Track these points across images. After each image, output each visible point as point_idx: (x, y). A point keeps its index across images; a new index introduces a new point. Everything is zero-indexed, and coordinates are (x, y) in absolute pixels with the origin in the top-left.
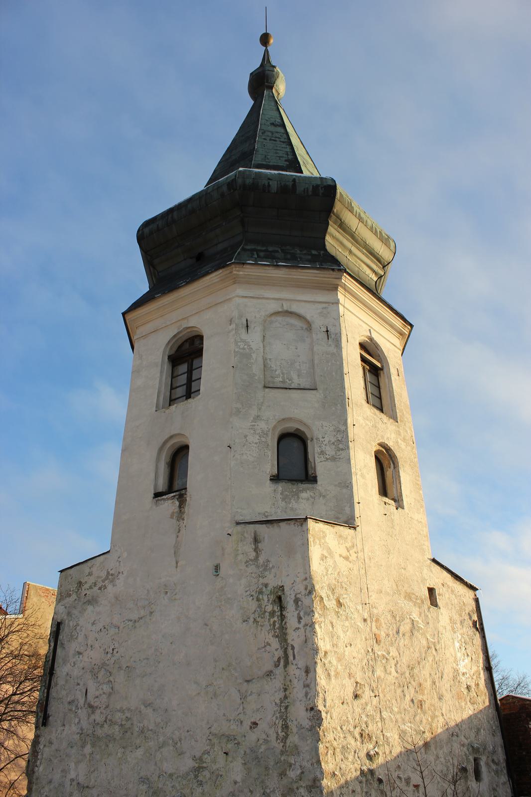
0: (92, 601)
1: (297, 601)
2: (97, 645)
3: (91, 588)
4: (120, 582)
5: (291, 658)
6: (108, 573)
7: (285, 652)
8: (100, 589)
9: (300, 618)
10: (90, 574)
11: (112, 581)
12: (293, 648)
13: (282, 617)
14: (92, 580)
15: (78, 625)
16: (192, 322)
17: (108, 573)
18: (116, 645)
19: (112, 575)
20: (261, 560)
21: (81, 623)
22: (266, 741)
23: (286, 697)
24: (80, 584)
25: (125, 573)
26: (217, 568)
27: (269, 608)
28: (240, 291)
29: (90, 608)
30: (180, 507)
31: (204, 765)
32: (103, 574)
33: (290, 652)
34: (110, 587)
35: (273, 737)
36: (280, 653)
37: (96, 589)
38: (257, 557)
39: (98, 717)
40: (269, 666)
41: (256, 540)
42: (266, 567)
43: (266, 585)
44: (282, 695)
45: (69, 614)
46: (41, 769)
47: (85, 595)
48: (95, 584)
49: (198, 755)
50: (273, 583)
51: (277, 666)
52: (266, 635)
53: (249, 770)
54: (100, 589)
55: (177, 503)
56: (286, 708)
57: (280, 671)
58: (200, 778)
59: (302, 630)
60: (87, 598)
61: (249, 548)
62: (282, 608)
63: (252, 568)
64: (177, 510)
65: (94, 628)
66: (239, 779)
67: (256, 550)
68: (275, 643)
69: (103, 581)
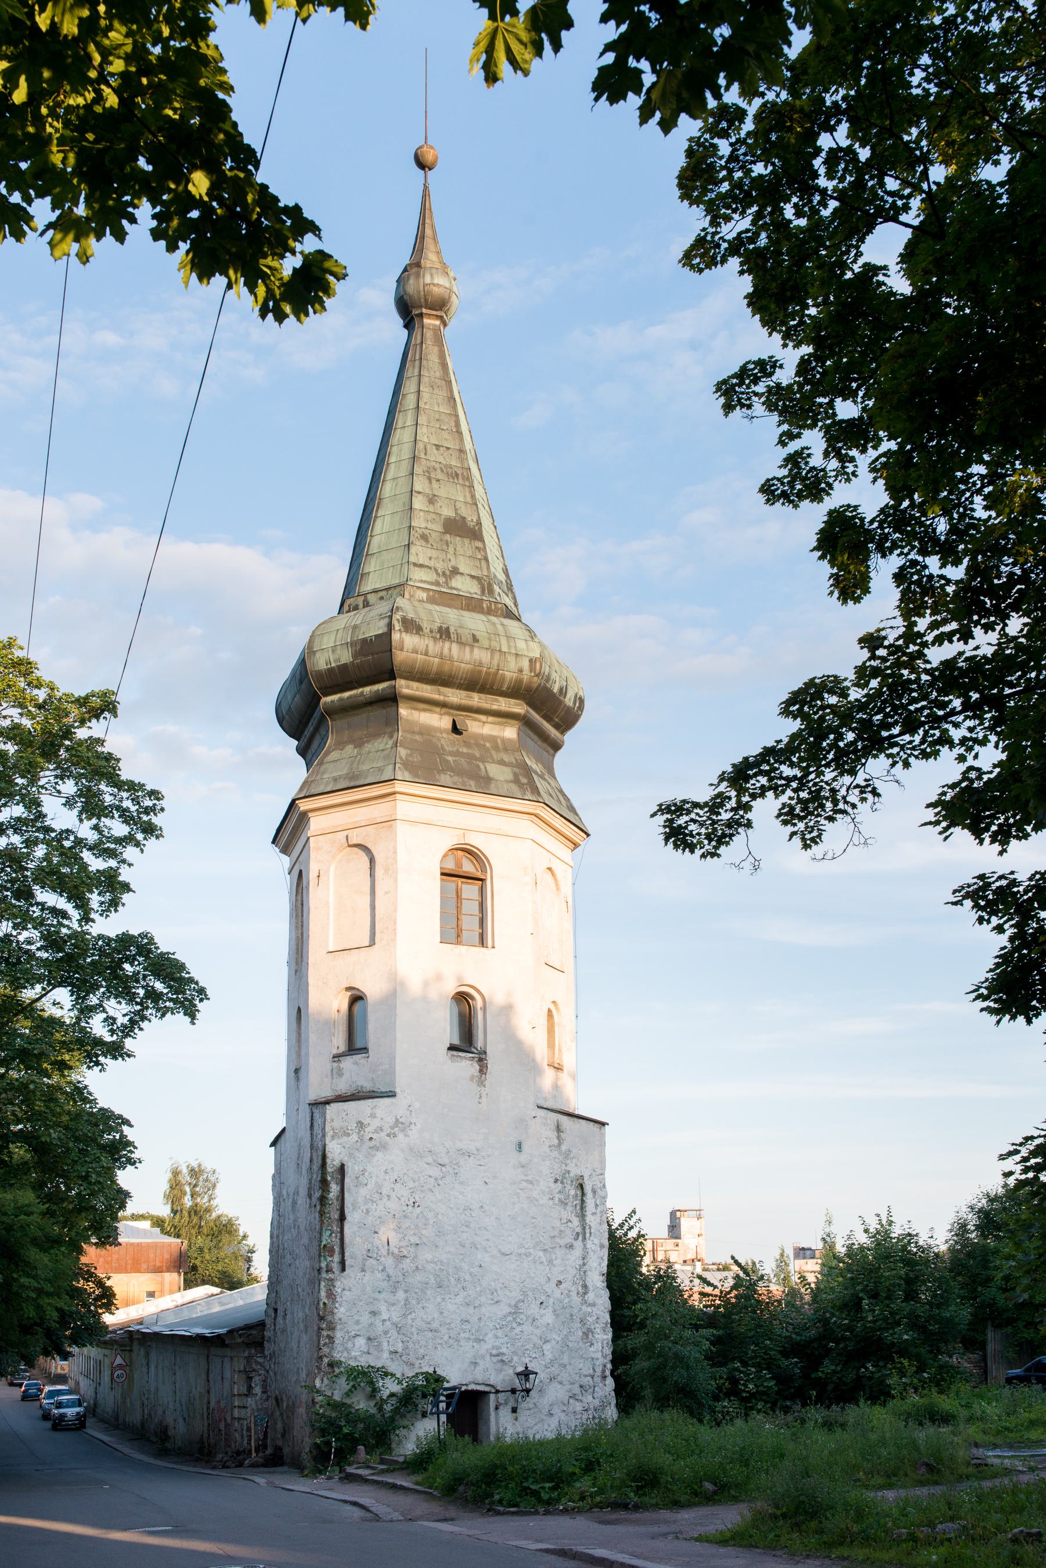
0: (383, 1147)
2: (393, 1195)
3: (376, 1131)
4: (414, 1132)
5: (588, 1235)
6: (397, 1120)
7: (584, 1229)
8: (388, 1135)
9: (597, 1205)
10: (373, 1116)
11: (403, 1131)
12: (590, 1228)
13: (583, 1201)
14: (375, 1123)
15: (364, 1170)
16: (476, 841)
17: (397, 1120)
18: (418, 1199)
19: (402, 1123)
20: (564, 1148)
21: (369, 1168)
22: (569, 1296)
23: (584, 1264)
24: (361, 1125)
25: (419, 1126)
26: (520, 1145)
27: (572, 1192)
29: (379, 1155)
30: (481, 1071)
32: (391, 1120)
33: (587, 1231)
34: (401, 1136)
35: (574, 1294)
36: (579, 1230)
37: (383, 1134)
38: (560, 1144)
39: (407, 1264)
40: (569, 1239)
41: (559, 1129)
42: (567, 1155)
43: (569, 1172)
44: (581, 1262)
45: (351, 1155)
46: (342, 1310)
47: (371, 1139)
48: (382, 1130)
49: (513, 1303)
50: (575, 1172)
51: (576, 1239)
52: (568, 1212)
53: (557, 1316)
54: (388, 1135)
55: (478, 1067)
56: (585, 1272)
57: (578, 1244)
58: (518, 1320)
59: (599, 1215)
60: (373, 1143)
62: (583, 1194)
63: (555, 1154)
64: (477, 1074)
65: (387, 1178)
66: (550, 1322)
67: (558, 1137)
68: (576, 1222)
69: (392, 1128)
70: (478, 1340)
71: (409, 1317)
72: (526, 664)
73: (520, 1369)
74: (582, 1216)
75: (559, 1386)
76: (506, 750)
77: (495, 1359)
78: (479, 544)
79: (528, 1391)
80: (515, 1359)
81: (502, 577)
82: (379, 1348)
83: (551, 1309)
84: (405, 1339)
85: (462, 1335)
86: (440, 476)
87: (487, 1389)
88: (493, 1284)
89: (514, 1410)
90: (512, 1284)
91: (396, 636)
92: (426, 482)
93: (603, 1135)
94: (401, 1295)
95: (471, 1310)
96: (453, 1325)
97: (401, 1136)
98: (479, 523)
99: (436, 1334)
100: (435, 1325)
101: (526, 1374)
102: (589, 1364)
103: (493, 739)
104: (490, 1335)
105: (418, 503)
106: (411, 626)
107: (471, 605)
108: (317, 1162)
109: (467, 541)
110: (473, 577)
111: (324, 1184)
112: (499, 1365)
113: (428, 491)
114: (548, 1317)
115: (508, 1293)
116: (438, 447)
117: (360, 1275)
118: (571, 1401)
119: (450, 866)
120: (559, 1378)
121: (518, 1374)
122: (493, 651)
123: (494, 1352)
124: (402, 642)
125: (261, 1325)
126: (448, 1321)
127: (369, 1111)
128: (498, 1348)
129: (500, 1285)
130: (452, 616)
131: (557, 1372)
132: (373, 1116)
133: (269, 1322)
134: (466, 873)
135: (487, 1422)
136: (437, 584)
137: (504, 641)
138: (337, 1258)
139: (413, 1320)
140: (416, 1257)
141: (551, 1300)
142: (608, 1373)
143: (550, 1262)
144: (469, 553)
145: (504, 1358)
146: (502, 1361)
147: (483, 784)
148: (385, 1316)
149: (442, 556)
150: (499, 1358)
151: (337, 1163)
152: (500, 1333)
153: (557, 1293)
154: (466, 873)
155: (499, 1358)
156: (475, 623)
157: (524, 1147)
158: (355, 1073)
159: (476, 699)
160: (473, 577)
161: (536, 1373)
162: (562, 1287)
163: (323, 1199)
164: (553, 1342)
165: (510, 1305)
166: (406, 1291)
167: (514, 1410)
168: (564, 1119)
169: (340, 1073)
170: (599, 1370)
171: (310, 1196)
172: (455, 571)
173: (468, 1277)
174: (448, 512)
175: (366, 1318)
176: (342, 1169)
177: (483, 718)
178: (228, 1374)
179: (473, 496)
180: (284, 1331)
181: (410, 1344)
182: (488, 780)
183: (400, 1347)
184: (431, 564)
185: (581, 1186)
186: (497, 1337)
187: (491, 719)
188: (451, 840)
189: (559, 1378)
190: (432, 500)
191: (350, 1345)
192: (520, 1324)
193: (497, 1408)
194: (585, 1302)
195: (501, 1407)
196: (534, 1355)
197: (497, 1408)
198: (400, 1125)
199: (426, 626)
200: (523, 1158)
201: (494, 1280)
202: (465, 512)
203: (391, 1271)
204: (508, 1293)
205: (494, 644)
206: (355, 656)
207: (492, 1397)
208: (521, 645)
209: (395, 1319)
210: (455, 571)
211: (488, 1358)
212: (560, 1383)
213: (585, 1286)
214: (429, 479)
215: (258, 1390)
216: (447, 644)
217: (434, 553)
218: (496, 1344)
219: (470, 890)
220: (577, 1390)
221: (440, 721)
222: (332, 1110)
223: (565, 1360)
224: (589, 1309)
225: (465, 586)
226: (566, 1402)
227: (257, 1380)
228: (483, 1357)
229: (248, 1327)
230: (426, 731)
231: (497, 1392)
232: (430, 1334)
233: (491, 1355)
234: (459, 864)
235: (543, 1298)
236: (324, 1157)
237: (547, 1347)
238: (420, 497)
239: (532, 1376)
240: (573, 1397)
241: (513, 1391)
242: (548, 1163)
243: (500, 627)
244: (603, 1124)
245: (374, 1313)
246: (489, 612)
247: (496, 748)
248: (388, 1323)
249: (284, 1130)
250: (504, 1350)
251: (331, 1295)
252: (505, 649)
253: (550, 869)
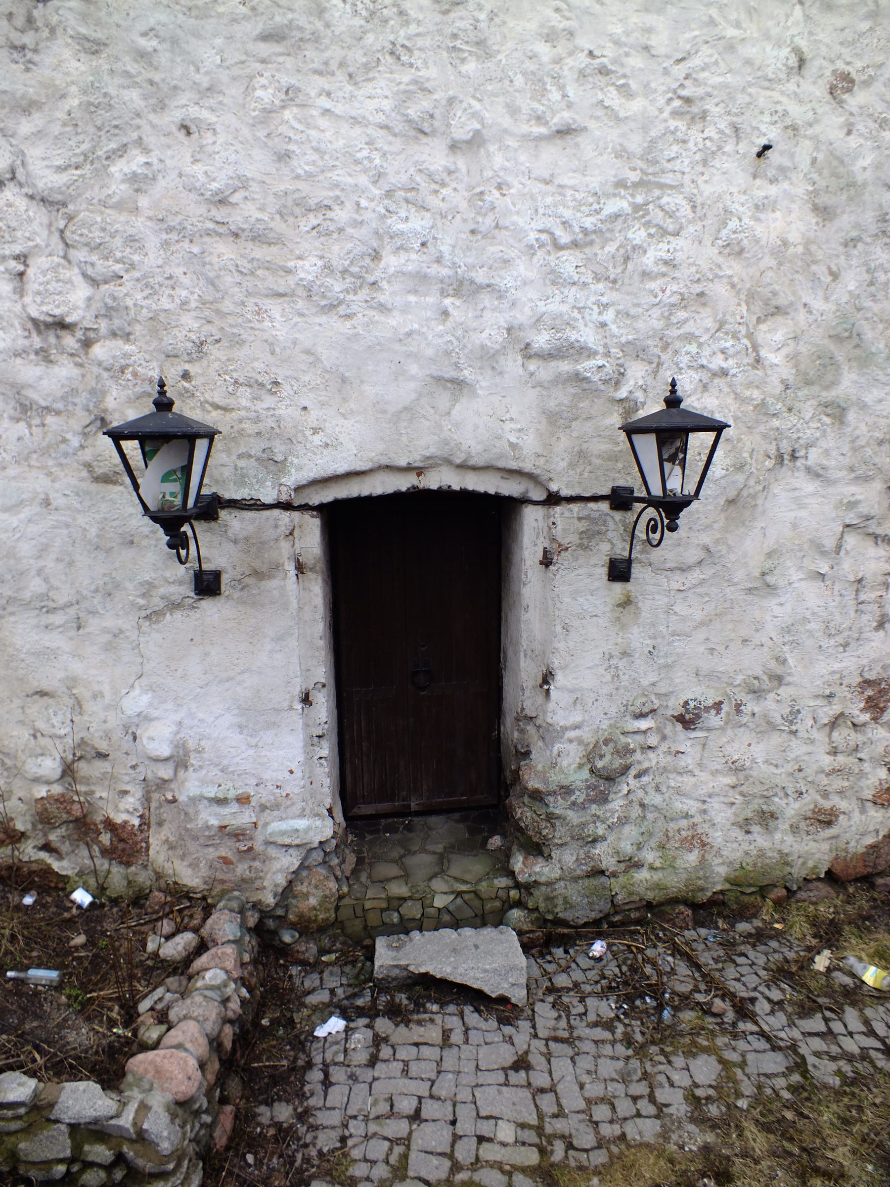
31: (668, 179)
70: (463, 288)
71: (119, 168)
75: (809, 486)
77: (545, 371)
79: (672, 507)
80: (637, 373)
83: (801, 189)
84: (102, 267)
85: (391, 261)
87: (510, 488)
88: (543, 50)
89: (619, 571)
90: (636, 61)
95: (434, 155)
96: (342, 215)
99: (261, 253)
100: (246, 213)
101: (672, 429)
104: (523, 269)
112: (561, 397)
114: (790, 223)
115: (613, 98)
118: (851, 540)
120: (814, 457)
123: (541, 340)
126: (322, 194)
128: (558, 324)
129: (582, 60)
131: (809, 433)
139: (139, 182)
141: (804, 153)
145: (587, 366)
146: (578, 378)
150: (565, 367)
152: (568, 263)
155: (565, 367)
161: (718, 428)
162: (856, 100)
164: (802, 316)
165: (621, 153)
167: (619, 571)
183: (76, 301)
189: (814, 457)
192: (664, 232)
195: (562, 560)
196: (718, 362)
197: (547, 561)
201: (550, 37)
204: (613, 98)
207: (532, 520)
209: (47, 179)
211: (513, 364)
212: (814, 473)
218: (554, 307)
226: (829, 543)
228: (488, 358)
231: (553, 499)
232: (224, 252)
233: (527, 352)
235: (772, 134)
237: (774, 337)
239: (699, 441)
250: (588, 336)
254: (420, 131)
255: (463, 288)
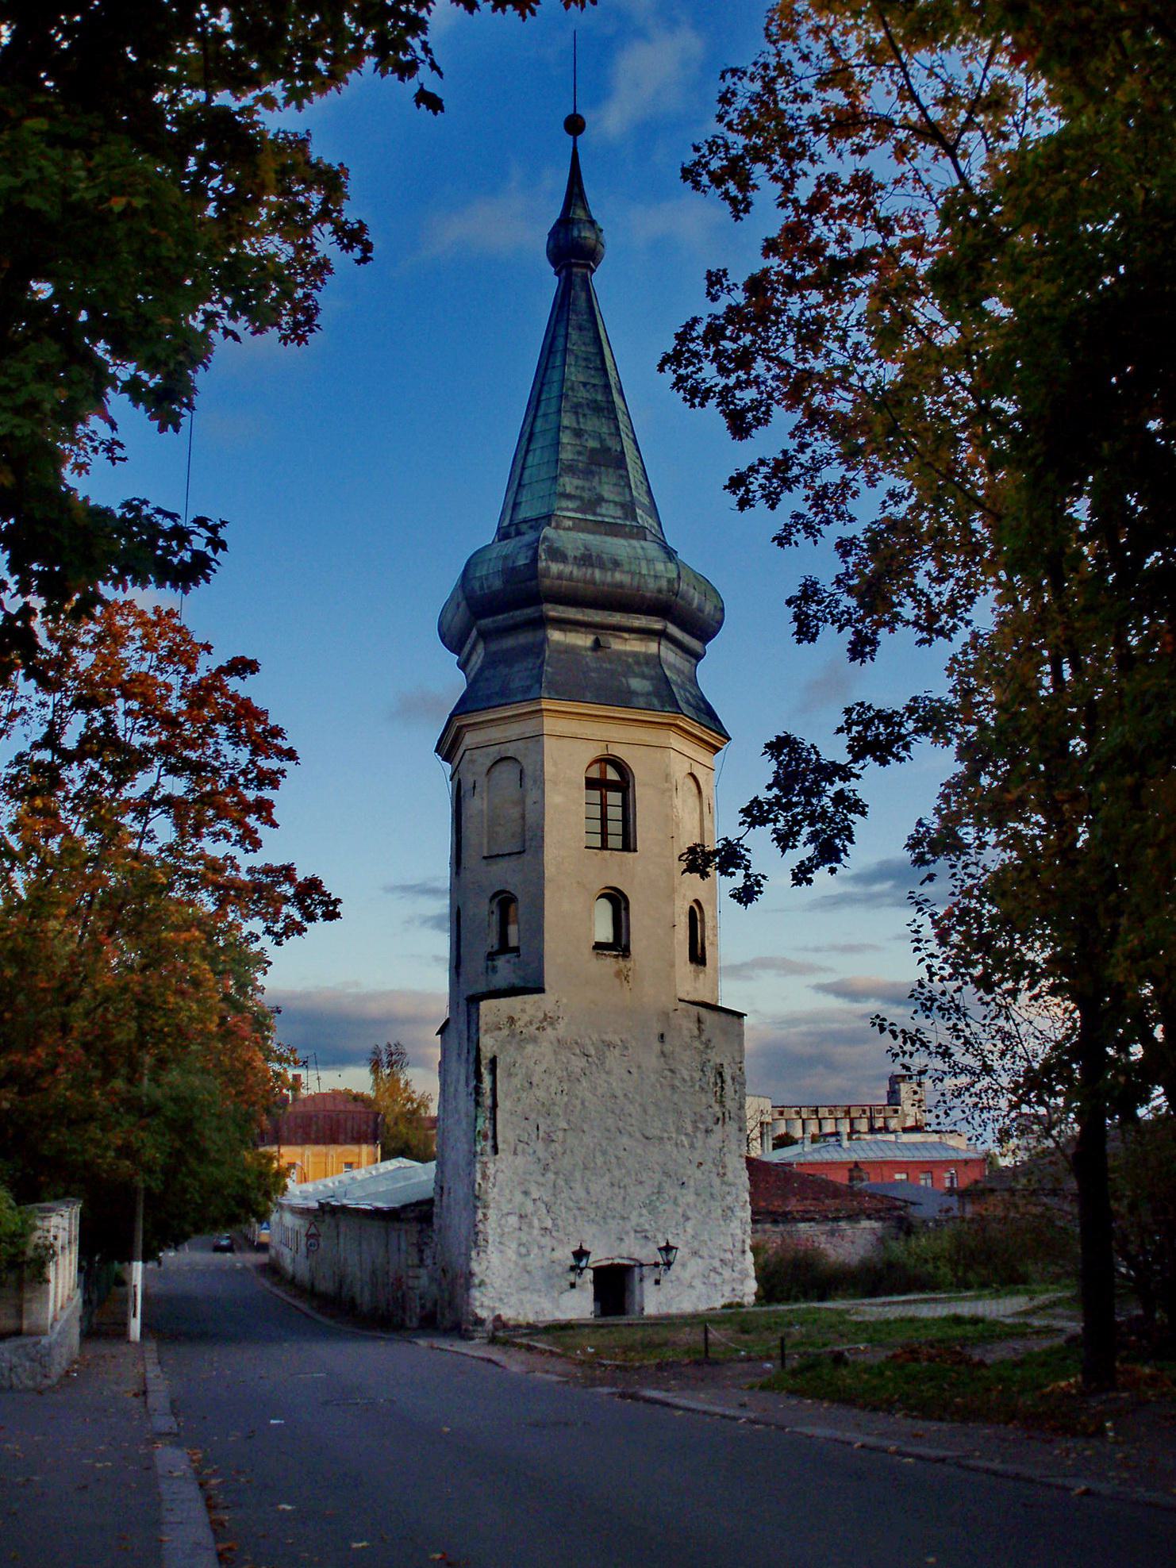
0: (534, 1040)
1: (733, 1079)
4: (561, 1026)
11: (551, 1024)
13: (722, 1088)
14: (526, 1018)
16: (618, 751)
20: (703, 1039)
26: (662, 1036)
27: (712, 1080)
28: (676, 741)
29: (530, 1048)
34: (549, 1030)
37: (533, 1028)
41: (699, 1021)
53: (698, 1195)
61: (694, 1027)
62: (723, 1082)
63: (697, 1044)
68: (717, 1108)
70: (623, 1218)
72: (664, 584)
73: (663, 1244)
74: (722, 1103)
76: (647, 664)
78: (622, 472)
81: (646, 500)
82: (531, 1226)
83: (692, 1190)
86: (587, 411)
89: (657, 1282)
91: (542, 565)
92: (574, 418)
93: (742, 1025)
94: (550, 1176)
97: (549, 1030)
98: (623, 452)
101: (668, 1249)
102: (730, 1239)
103: (635, 654)
104: (635, 1213)
105: (566, 438)
106: (557, 555)
107: (613, 530)
108: (473, 1053)
109: (611, 470)
110: (615, 503)
111: (478, 1076)
112: (643, 1241)
113: (575, 425)
116: (585, 384)
117: (511, 1158)
119: (595, 773)
121: (660, 1249)
122: (632, 573)
124: (548, 568)
125: (430, 1202)
127: (519, 1008)
130: (595, 541)
132: (523, 1011)
133: (437, 1198)
134: (612, 781)
135: (633, 1292)
136: (583, 512)
137: (643, 563)
138: (490, 1143)
140: (564, 1141)
142: (747, 1248)
143: (692, 1146)
144: (614, 480)
147: (623, 698)
148: (535, 1195)
149: (587, 485)
151: (489, 1055)
153: (698, 1174)
154: (612, 781)
156: (618, 547)
157: (667, 1039)
158: (505, 971)
159: (617, 618)
160: (615, 503)
163: (478, 1090)
166: (556, 1173)
167: (657, 1282)
168: (703, 1011)
169: (494, 969)
170: (739, 1245)
171: (467, 1085)
172: (600, 500)
173: (613, 1160)
174: (592, 444)
175: (519, 1197)
176: (493, 1061)
177: (626, 635)
178: (403, 1246)
179: (618, 428)
180: (449, 1208)
181: (560, 1222)
182: (632, 693)
183: (549, 1224)
184: (578, 493)
185: (721, 1074)
186: (641, 1215)
187: (633, 636)
188: (597, 751)
190: (578, 433)
191: (503, 1222)
193: (641, 1280)
194: (723, 1183)
198: (549, 1020)
199: (570, 553)
200: (667, 1048)
202: (611, 443)
203: (540, 1154)
205: (634, 567)
206: (506, 582)
207: (637, 1270)
208: (660, 567)
210: (600, 500)
211: (632, 1234)
213: (724, 1167)
214: (576, 413)
215: (429, 1262)
216: (589, 571)
217: (579, 483)
219: (614, 798)
220: (717, 1264)
221: (583, 640)
222: (484, 1005)
223: (706, 1237)
224: (727, 1189)
225: (610, 513)
227: (428, 1253)
229: (419, 1203)
230: (571, 650)
231: (642, 1265)
234: (603, 772)
236: (478, 1050)
237: (689, 1225)
238: (568, 432)
240: (714, 1270)
241: (657, 1265)
242: (688, 1053)
243: (639, 551)
244: (741, 1015)
245: (526, 1193)
246: (629, 536)
247: (638, 663)
248: (539, 1203)
249: (448, 1021)
250: (647, 1227)
251: (484, 1177)
252: (644, 571)
253: (691, 774)
254: (612, 1185)
255: (623, 1218)
